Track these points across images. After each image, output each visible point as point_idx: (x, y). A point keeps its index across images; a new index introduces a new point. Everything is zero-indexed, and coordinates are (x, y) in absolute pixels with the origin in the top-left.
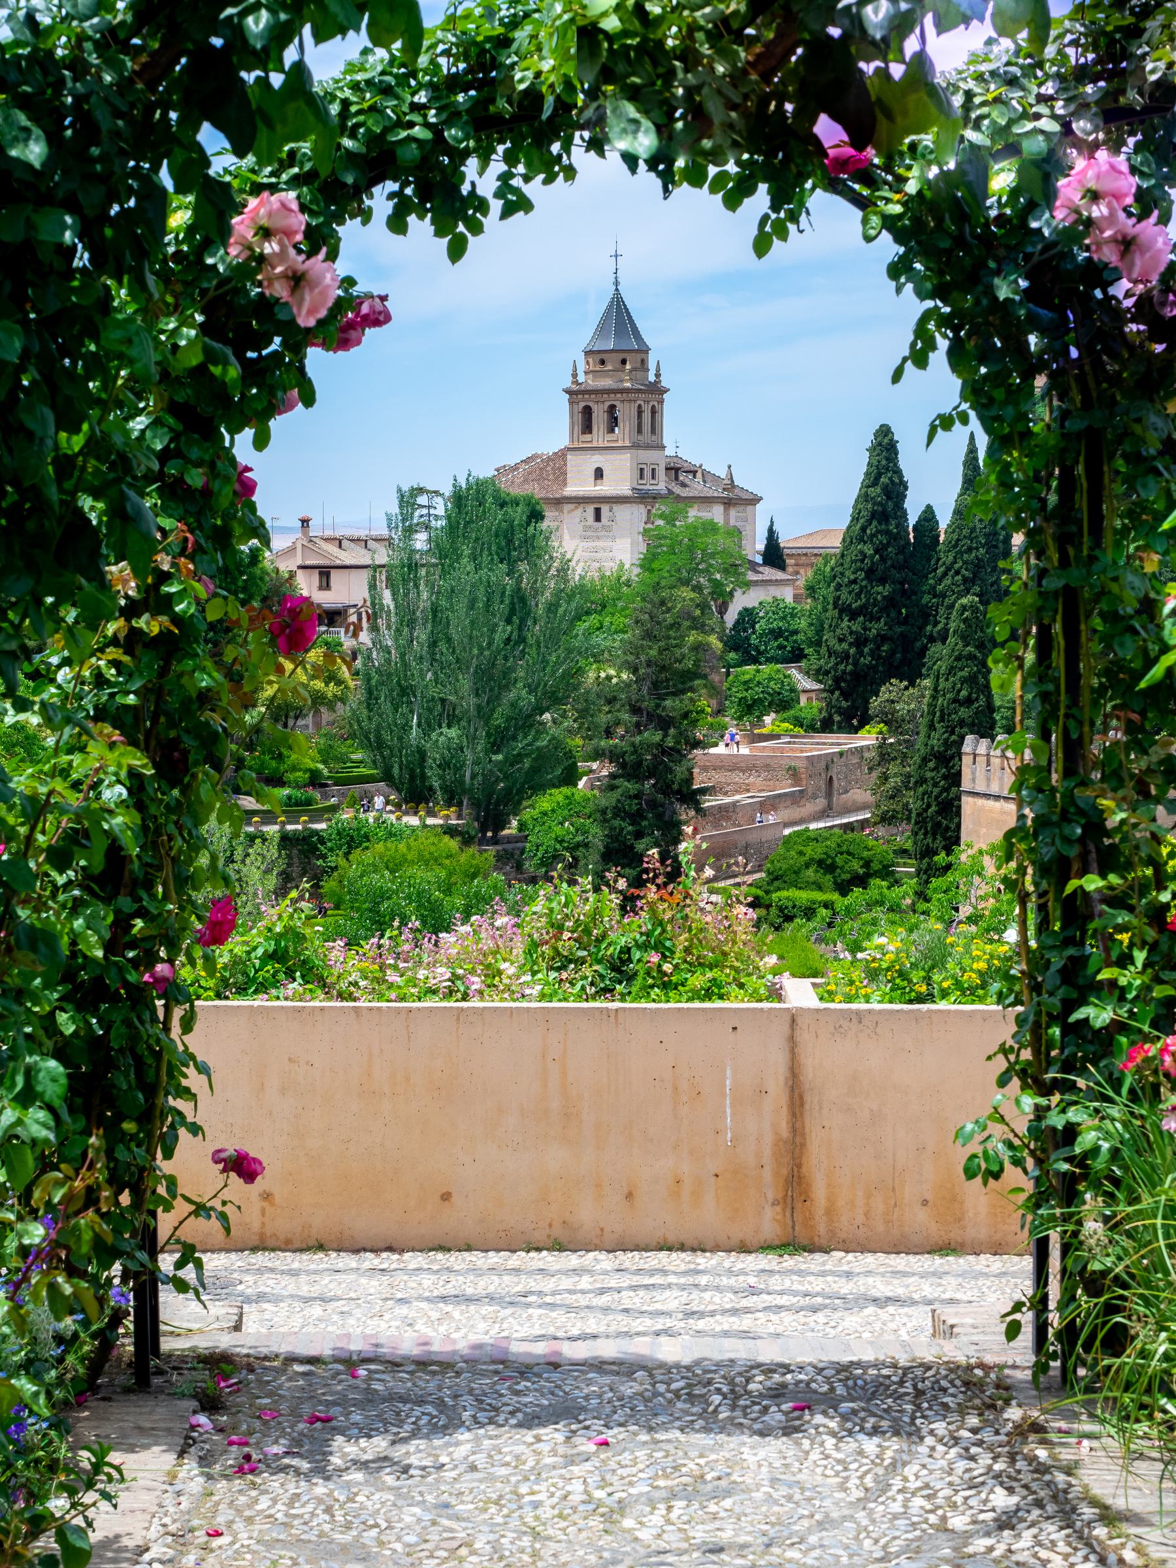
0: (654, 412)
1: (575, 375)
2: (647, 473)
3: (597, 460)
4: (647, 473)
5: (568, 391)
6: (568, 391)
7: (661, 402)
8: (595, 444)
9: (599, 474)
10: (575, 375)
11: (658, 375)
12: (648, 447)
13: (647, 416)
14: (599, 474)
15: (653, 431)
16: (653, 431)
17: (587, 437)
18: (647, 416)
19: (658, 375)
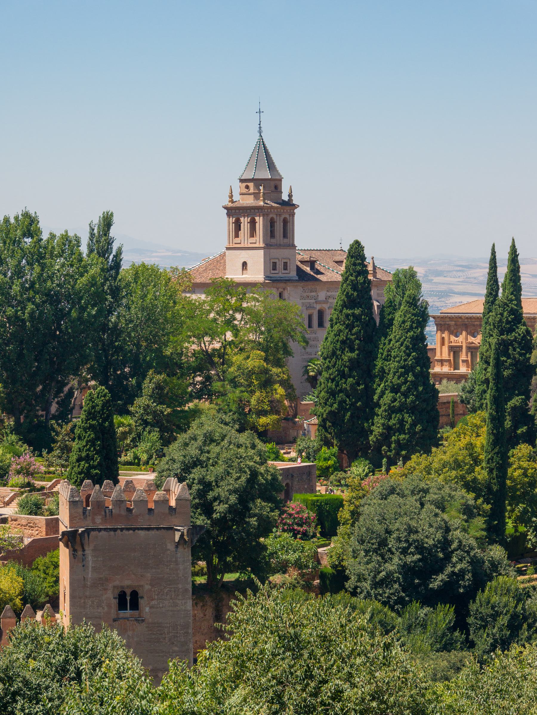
0: (285, 222)
1: (231, 196)
2: (280, 266)
3: (244, 256)
4: (280, 266)
5: (225, 208)
6: (225, 208)
7: (293, 215)
8: (242, 246)
9: (245, 264)
10: (231, 196)
11: (290, 196)
12: (279, 246)
13: (279, 227)
14: (245, 264)
15: (285, 236)
16: (285, 236)
17: (237, 240)
18: (279, 227)
19: (290, 196)
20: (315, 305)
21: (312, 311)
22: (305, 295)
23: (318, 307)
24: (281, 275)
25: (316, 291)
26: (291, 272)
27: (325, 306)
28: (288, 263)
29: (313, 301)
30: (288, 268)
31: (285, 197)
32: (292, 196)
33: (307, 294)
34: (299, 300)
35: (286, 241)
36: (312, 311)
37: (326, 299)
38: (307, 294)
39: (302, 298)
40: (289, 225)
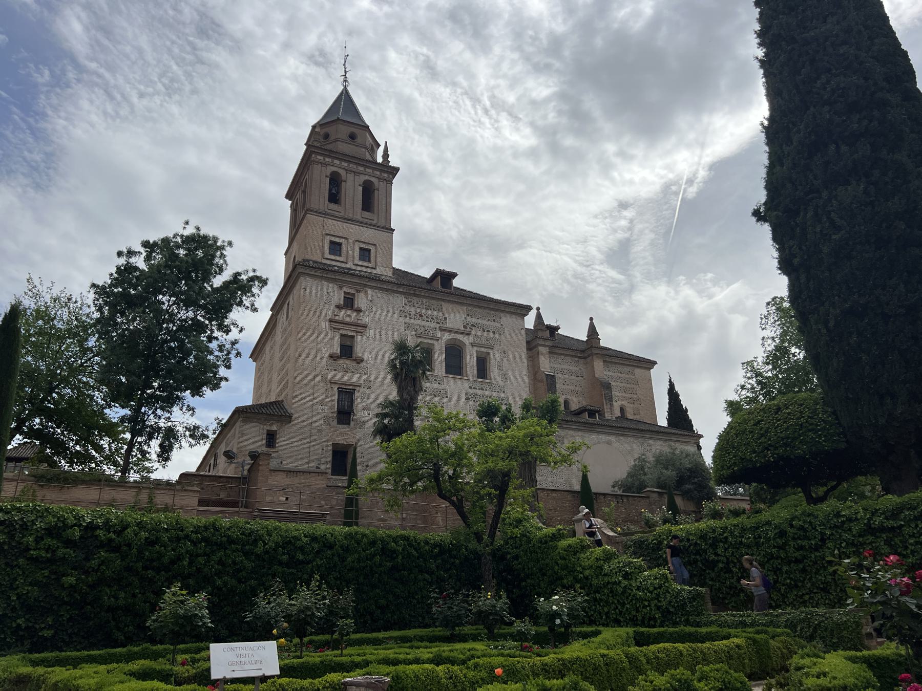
19: (386, 155)
20: (438, 334)
21: (431, 342)
22: (413, 310)
23: (446, 337)
24: (350, 265)
25: (440, 310)
26: (378, 268)
27: (466, 340)
28: (373, 251)
29: (432, 325)
30: (372, 259)
31: (380, 160)
32: (388, 155)
33: (419, 310)
34: (397, 316)
35: (367, 214)
36: (431, 342)
37: (465, 327)
38: (419, 310)
39: (404, 314)
40: (378, 196)
